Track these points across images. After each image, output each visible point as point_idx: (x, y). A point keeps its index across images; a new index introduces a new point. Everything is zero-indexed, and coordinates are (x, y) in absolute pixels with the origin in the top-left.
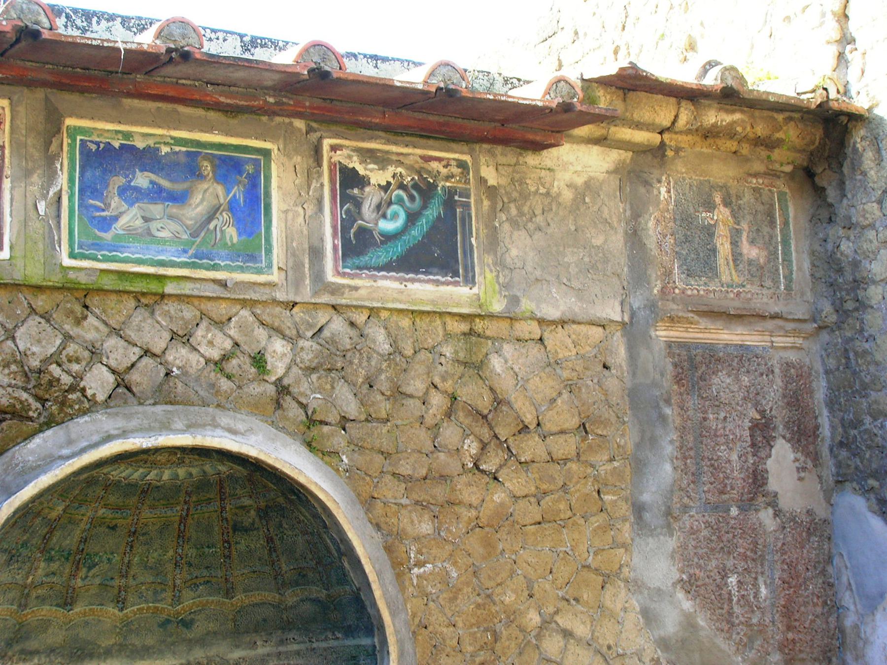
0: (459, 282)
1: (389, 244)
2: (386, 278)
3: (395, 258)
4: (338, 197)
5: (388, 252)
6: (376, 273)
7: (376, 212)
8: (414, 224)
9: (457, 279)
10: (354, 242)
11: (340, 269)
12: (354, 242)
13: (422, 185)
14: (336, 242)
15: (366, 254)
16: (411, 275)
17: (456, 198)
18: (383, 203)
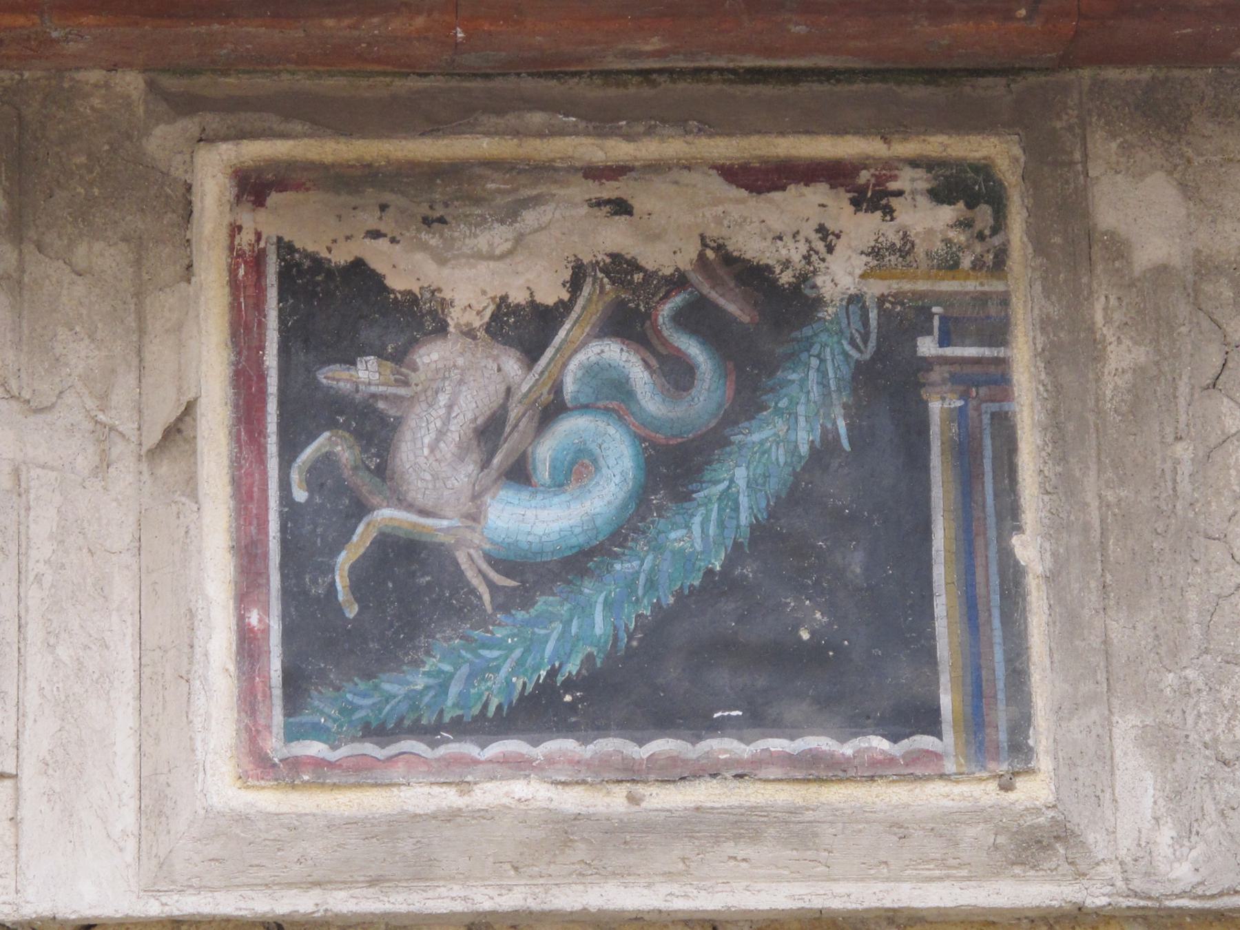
0: (937, 756)
1: (543, 603)
2: (518, 767)
3: (572, 667)
4: (272, 407)
5: (532, 645)
6: (469, 749)
7: (475, 456)
8: (687, 497)
9: (925, 742)
10: (352, 611)
11: (275, 745)
12: (352, 611)
13: (732, 308)
14: (254, 618)
15: (417, 663)
16: (663, 745)
17: (927, 347)
18: (513, 415)
